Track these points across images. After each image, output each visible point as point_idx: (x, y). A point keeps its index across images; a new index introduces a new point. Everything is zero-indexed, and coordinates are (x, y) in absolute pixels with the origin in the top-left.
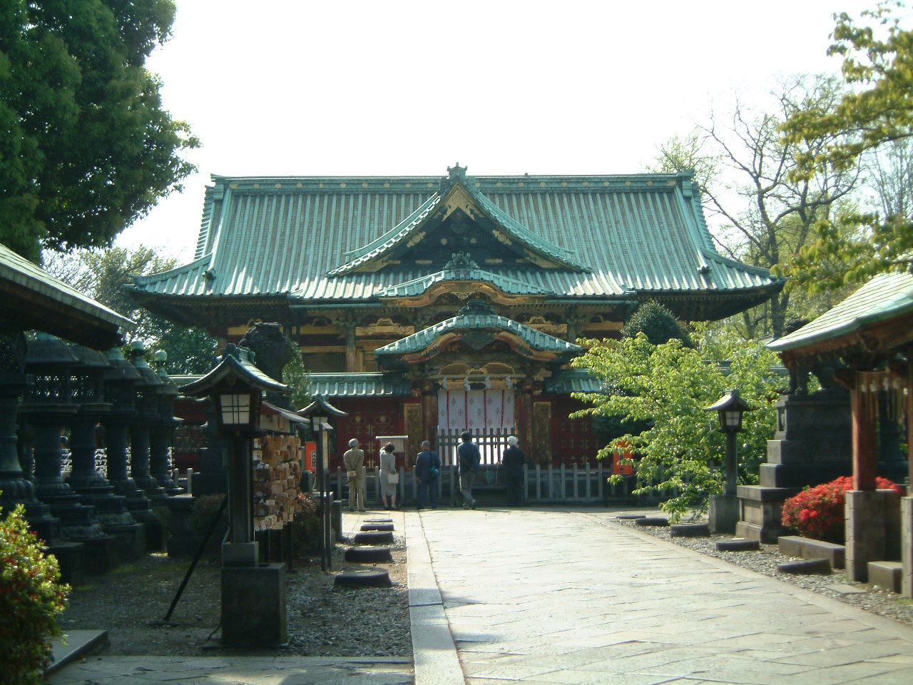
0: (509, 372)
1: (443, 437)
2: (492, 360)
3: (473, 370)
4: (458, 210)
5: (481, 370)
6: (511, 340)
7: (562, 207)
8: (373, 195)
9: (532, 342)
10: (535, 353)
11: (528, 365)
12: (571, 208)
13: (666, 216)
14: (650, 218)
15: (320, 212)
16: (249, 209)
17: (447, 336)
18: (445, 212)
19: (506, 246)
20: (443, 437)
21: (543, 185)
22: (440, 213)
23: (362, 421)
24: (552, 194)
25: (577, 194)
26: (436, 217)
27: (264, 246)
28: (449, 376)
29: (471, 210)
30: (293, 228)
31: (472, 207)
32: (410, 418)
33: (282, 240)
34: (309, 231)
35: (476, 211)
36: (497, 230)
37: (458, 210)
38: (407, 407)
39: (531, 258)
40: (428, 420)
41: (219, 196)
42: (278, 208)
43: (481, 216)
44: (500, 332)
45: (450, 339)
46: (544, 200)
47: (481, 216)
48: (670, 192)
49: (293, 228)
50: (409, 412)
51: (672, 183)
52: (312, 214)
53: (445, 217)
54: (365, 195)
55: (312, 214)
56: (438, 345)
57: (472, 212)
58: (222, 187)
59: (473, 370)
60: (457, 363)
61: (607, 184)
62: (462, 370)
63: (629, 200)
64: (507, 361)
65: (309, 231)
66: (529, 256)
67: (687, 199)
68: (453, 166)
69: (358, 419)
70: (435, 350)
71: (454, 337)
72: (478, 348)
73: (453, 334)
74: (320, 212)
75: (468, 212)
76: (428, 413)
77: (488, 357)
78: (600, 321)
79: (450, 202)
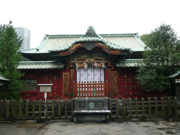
0: (102, 60)
1: (80, 84)
2: (95, 56)
3: (89, 60)
5: (92, 60)
6: (102, 46)
7: (113, 39)
8: (76, 38)
9: (111, 46)
10: (112, 51)
11: (109, 57)
12: (114, 39)
13: (134, 40)
14: (131, 40)
15: (65, 40)
16: (52, 40)
17: (77, 45)
20: (80, 84)
21: (109, 36)
23: (48, 79)
24: (110, 37)
25: (115, 37)
27: (52, 45)
28: (79, 62)
30: (59, 43)
32: (65, 78)
33: (56, 45)
34: (62, 43)
38: (64, 74)
40: (71, 78)
41: (46, 38)
42: (57, 40)
44: (98, 43)
45: (78, 46)
46: (109, 38)
48: (134, 37)
49: (59, 43)
50: (65, 75)
51: (134, 35)
52: (63, 41)
54: (74, 38)
55: (63, 41)
56: (73, 48)
58: (46, 36)
59: (89, 60)
60: (83, 57)
61: (121, 35)
62: (84, 60)
63: (126, 38)
64: (101, 57)
65: (62, 43)
67: (137, 37)
68: (90, 26)
69: (46, 78)
70: (72, 50)
71: (80, 45)
72: (89, 49)
73: (79, 44)
74: (65, 40)
76: (72, 76)
77: (94, 55)
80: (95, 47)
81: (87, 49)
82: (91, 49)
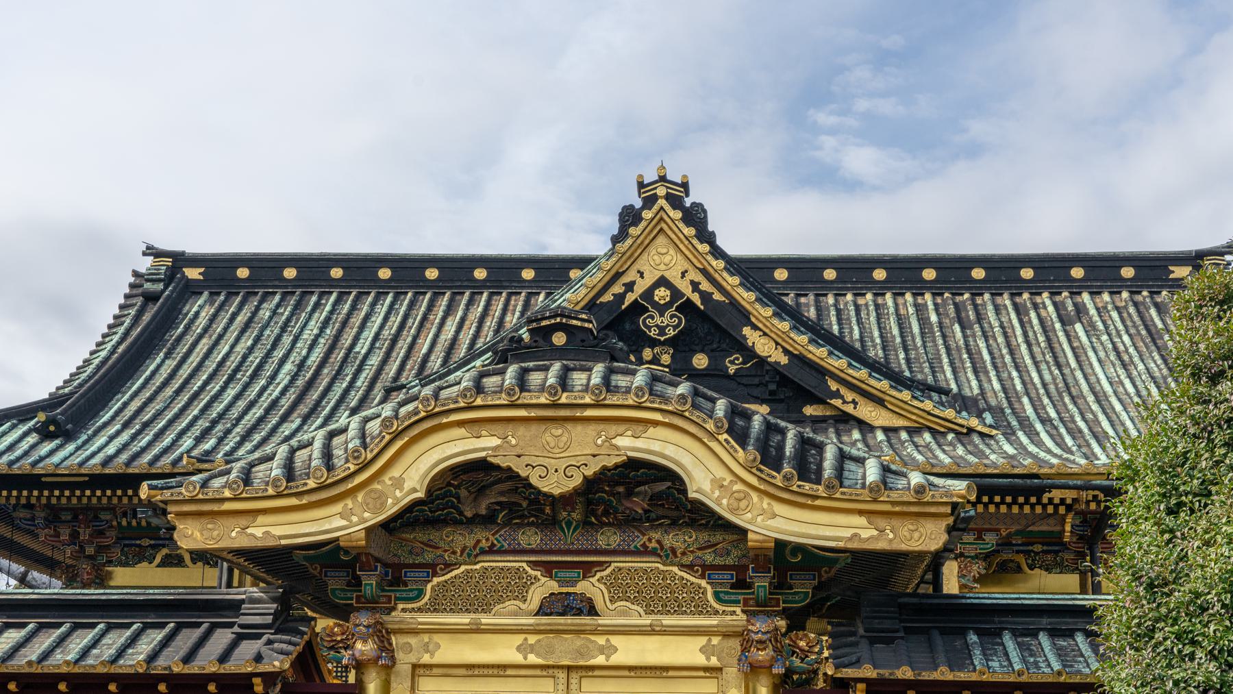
4: (662, 282)
18: (630, 287)
19: (775, 368)
22: (618, 289)
26: (607, 297)
29: (692, 282)
31: (698, 277)
35: (705, 286)
36: (755, 328)
37: (662, 282)
39: (845, 402)
43: (717, 296)
47: (717, 296)
53: (630, 298)
57: (695, 286)
66: (837, 394)
75: (686, 289)
77: (609, 538)
78: (1019, 569)
79: (642, 264)
80: (611, 462)
81: (534, 481)
82: (577, 481)
